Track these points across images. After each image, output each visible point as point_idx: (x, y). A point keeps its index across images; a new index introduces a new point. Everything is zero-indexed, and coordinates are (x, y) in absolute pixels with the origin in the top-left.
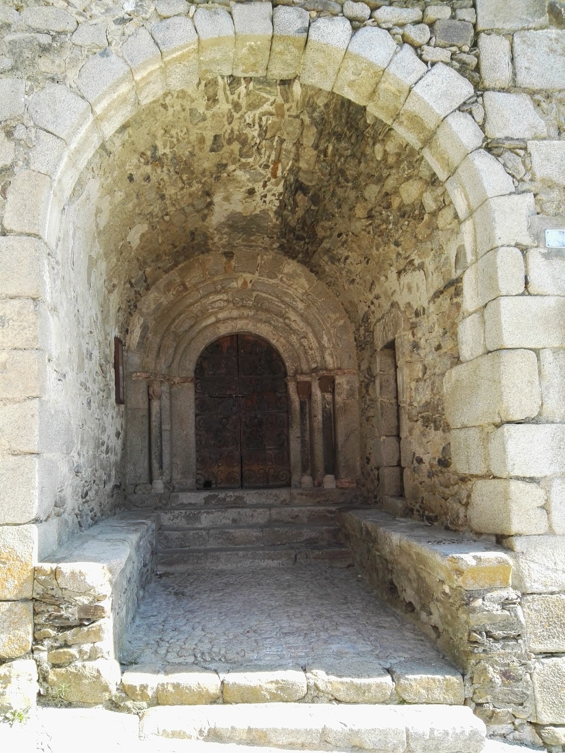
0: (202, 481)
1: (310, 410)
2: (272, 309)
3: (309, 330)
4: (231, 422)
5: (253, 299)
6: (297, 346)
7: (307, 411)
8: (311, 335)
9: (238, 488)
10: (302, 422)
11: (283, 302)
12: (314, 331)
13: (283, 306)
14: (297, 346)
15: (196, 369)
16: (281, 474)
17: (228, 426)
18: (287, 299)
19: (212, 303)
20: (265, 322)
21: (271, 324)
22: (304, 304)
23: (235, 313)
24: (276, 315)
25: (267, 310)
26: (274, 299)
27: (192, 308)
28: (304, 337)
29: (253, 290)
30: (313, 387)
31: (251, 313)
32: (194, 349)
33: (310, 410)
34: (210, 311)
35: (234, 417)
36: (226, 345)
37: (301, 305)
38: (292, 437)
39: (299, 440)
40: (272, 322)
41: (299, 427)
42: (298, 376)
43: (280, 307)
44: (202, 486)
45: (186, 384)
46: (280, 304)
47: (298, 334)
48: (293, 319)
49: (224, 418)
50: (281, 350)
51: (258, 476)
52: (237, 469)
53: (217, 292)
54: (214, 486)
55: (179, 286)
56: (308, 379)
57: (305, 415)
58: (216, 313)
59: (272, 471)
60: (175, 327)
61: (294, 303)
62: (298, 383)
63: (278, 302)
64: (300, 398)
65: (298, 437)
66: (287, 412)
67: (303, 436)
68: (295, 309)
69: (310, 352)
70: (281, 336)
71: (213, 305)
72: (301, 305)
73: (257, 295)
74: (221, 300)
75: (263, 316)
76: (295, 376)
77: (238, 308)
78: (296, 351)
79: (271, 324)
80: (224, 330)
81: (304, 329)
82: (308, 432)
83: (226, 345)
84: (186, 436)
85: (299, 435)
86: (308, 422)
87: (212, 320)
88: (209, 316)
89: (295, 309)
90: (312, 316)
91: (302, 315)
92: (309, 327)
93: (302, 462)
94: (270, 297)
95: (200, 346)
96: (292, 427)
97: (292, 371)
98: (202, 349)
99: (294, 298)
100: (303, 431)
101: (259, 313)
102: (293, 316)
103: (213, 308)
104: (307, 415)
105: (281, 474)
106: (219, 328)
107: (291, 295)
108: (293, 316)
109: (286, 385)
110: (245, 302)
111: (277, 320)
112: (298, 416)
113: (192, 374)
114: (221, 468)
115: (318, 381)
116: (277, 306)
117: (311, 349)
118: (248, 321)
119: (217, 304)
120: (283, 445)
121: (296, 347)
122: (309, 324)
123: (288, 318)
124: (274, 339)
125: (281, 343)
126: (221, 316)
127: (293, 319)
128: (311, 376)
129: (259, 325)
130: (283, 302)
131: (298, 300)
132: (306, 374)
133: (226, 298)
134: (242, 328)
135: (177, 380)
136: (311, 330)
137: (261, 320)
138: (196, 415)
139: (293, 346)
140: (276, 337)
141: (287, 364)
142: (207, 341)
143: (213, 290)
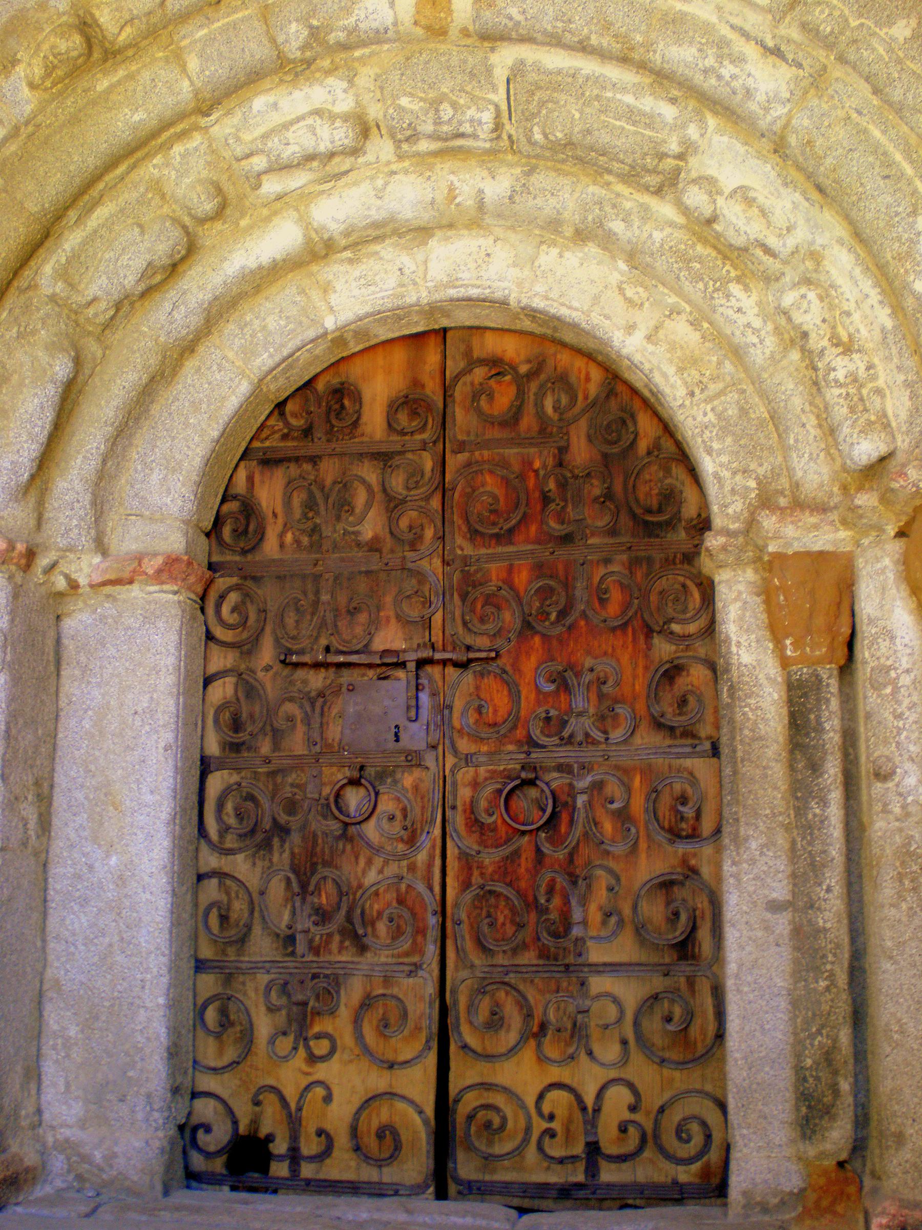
0: (218, 1137)
1: (850, 738)
2: (604, 138)
3: (828, 233)
4: (386, 805)
5: (500, 97)
6: (763, 347)
7: (832, 735)
8: (841, 264)
9: (417, 1190)
10: (800, 811)
11: (662, 78)
12: (860, 237)
13: (669, 112)
14: (763, 347)
15: (218, 522)
16: (675, 1116)
17: (371, 830)
18: (680, 55)
19: (265, 136)
20: (581, 236)
21: (607, 241)
22: (785, 73)
23: (408, 195)
24: (631, 177)
25: (578, 155)
26: (613, 72)
27: (152, 168)
28: (807, 281)
29: (492, 37)
30: (868, 603)
31: (497, 186)
32: (195, 406)
33: (850, 738)
34: (271, 186)
35: (408, 780)
36: (378, 389)
37: (765, 82)
38: (734, 904)
39: (782, 923)
40: (617, 226)
41: (782, 840)
42: (769, 522)
43: (650, 120)
44: (218, 1165)
45: (135, 591)
46: (647, 103)
47: (768, 279)
48: (729, 179)
49: (354, 782)
50: (672, 386)
51: (540, 1125)
52: (418, 1083)
53: (288, 69)
54: (280, 1169)
55: (62, 31)
56: (827, 537)
57: (815, 767)
58: (304, 197)
59: (618, 1097)
60: (63, 274)
61: (727, 70)
62: (772, 566)
63: (637, 91)
64: (785, 662)
65: (775, 907)
66: (715, 751)
67: (801, 902)
68: (729, 111)
69: (842, 367)
70: (674, 311)
71: (274, 143)
72: (765, 82)
73: (517, 71)
74: (318, 112)
75: (566, 194)
76: (751, 523)
77: (424, 161)
78: (756, 380)
79: (607, 241)
80: (354, 297)
81: (801, 235)
82: (834, 878)
83: (378, 389)
84: (121, 881)
85: (780, 891)
86: (835, 812)
87: (280, 238)
88: (268, 219)
89: (729, 111)
90: (840, 133)
91: (779, 148)
92: (828, 216)
93: (799, 1071)
94: (588, 66)
95: (222, 389)
96: (738, 841)
97: (737, 506)
98: (233, 402)
99: (722, 44)
100: (805, 871)
101: (541, 180)
102: (727, 164)
103: (282, 167)
104: (832, 769)
105: (675, 1116)
106: (327, 288)
107: (707, 29)
108: (727, 164)
109: (708, 589)
110: (447, 111)
111: (646, 213)
112: (778, 772)
113: (175, 541)
114: (322, 1071)
115: (895, 547)
116: (631, 114)
117: (848, 348)
118: (486, 242)
119: (299, 141)
120: (687, 944)
121: (758, 357)
122: (823, 191)
123: (709, 183)
124: (631, 328)
125: (673, 347)
126: (335, 211)
127: (729, 179)
128: (851, 518)
129: (548, 257)
130: (662, 78)
131: (751, 51)
132: (822, 509)
133: (345, 104)
134: (451, 284)
135: (86, 567)
136: (840, 230)
137: (554, 225)
138: (206, 767)
139: (737, 353)
140: (645, 319)
141: (708, 465)
142: (264, 360)
143: (256, 50)
